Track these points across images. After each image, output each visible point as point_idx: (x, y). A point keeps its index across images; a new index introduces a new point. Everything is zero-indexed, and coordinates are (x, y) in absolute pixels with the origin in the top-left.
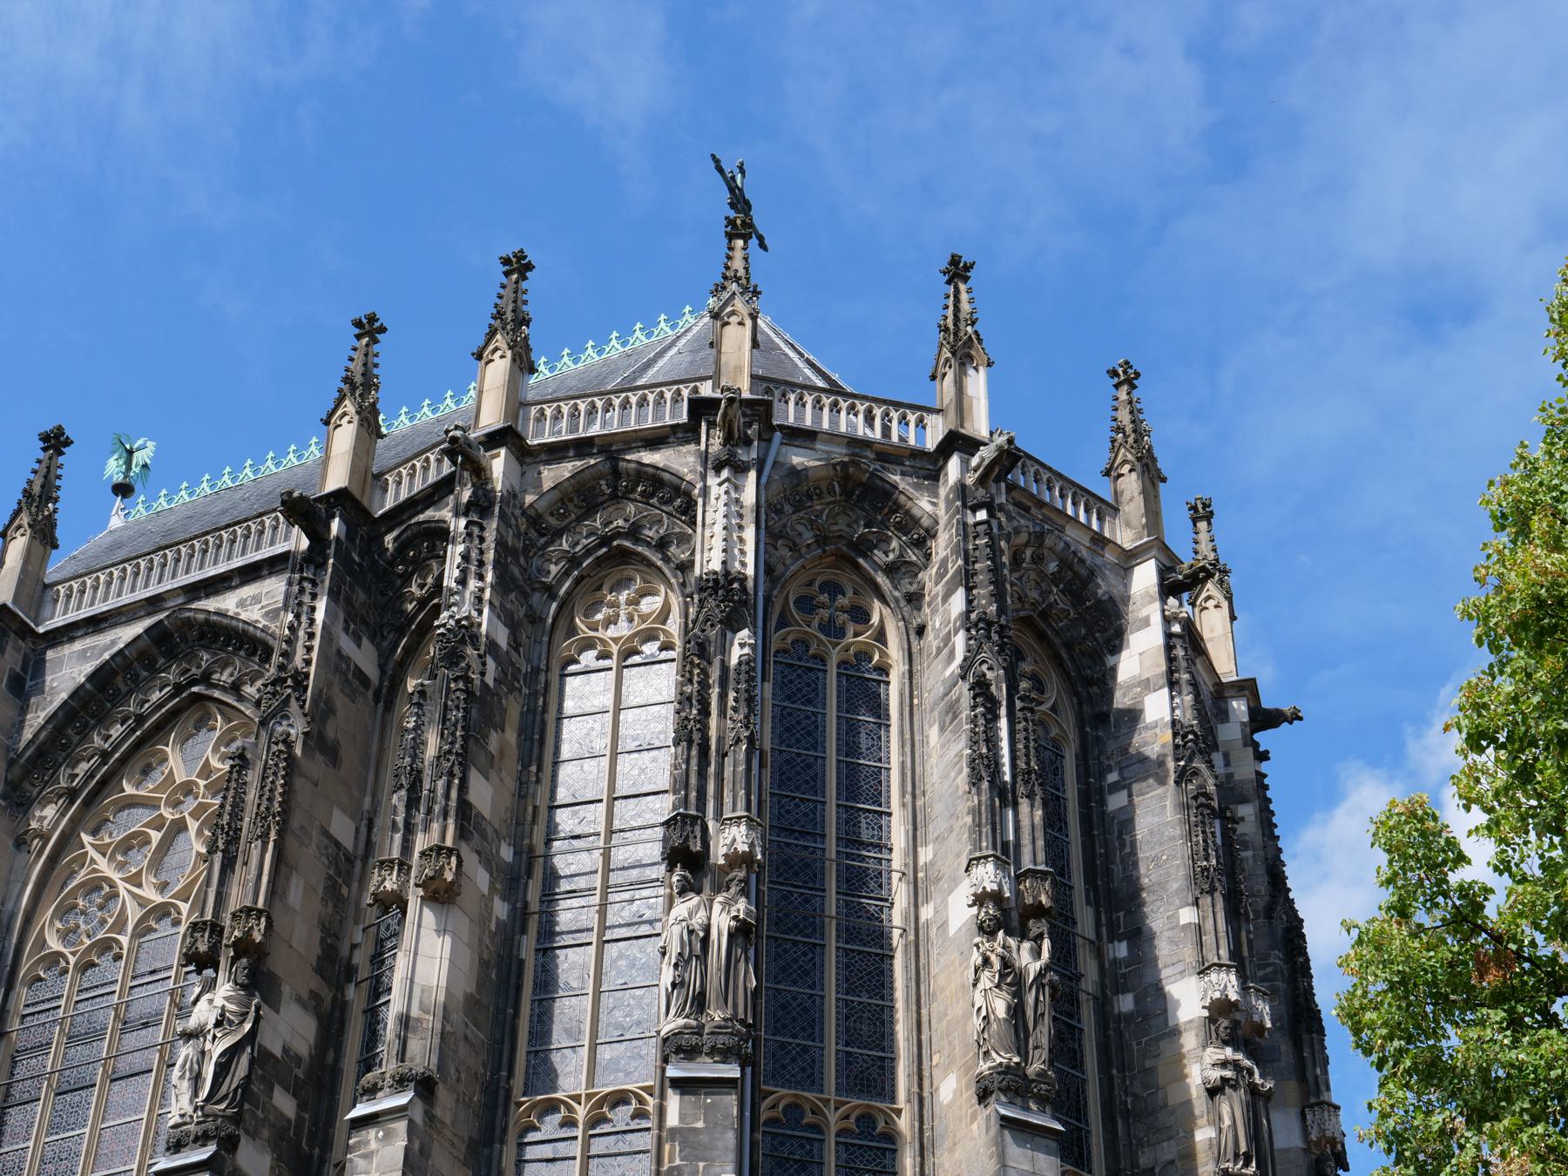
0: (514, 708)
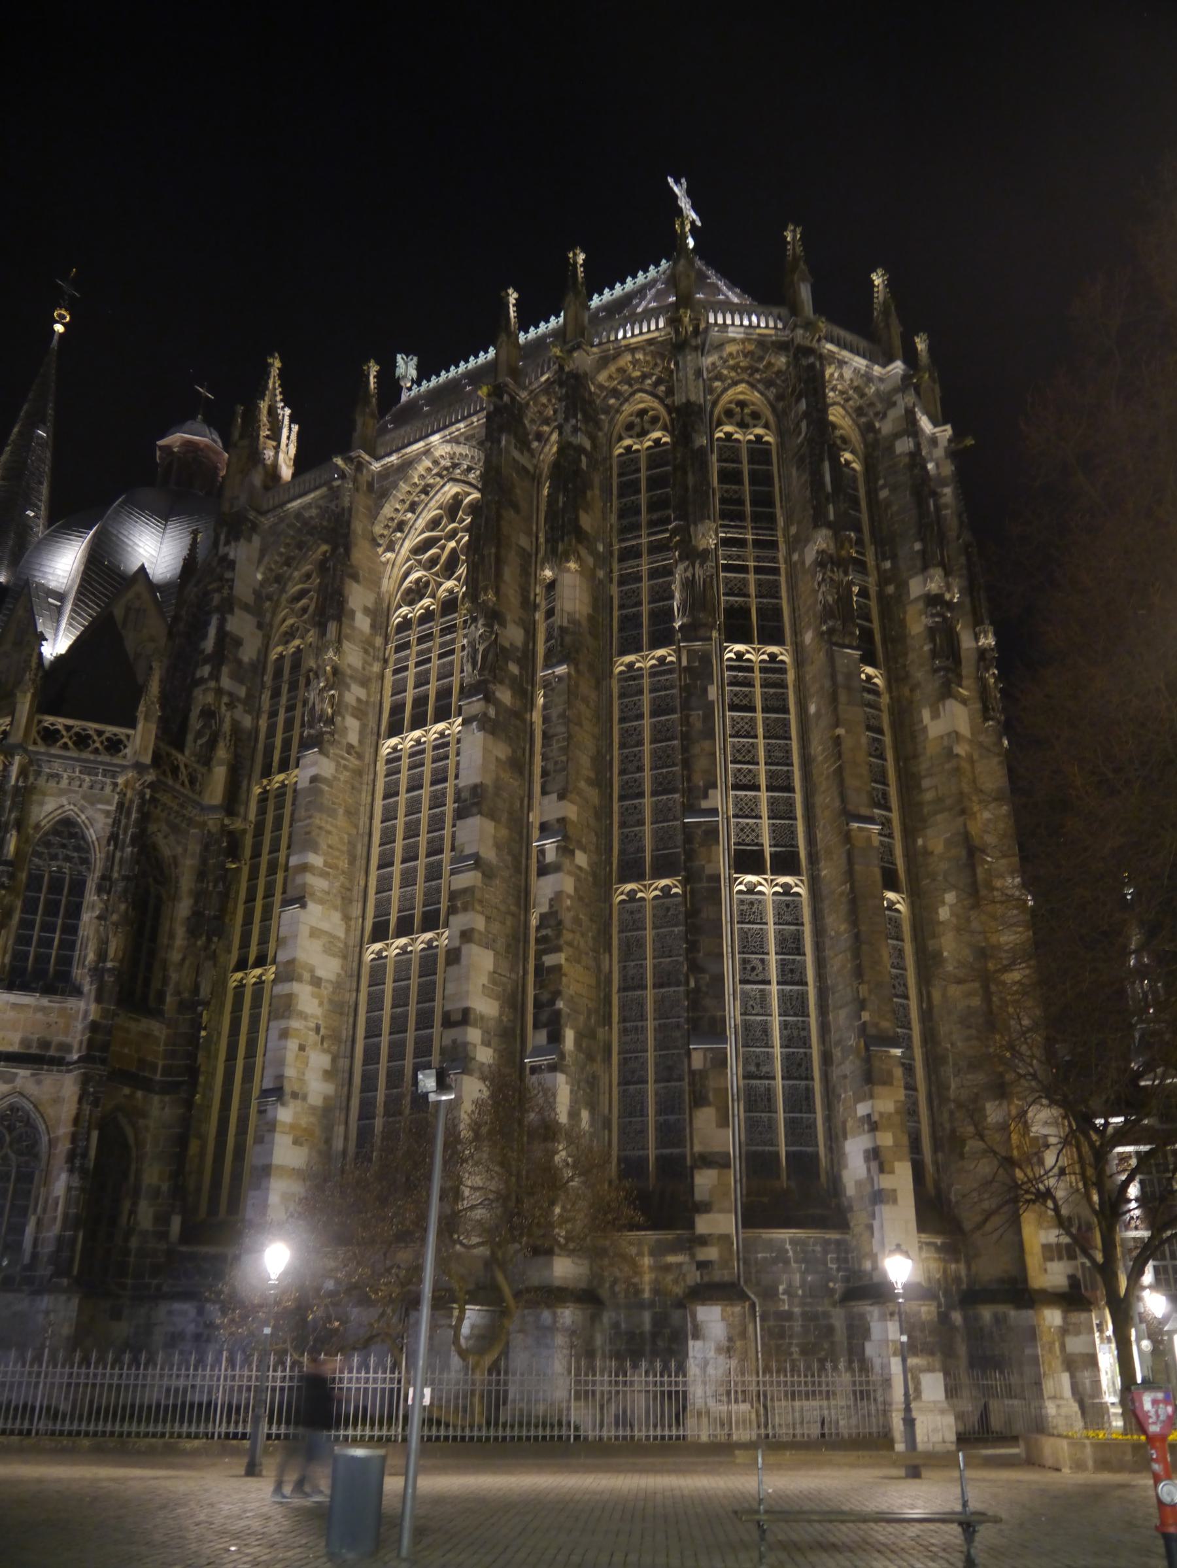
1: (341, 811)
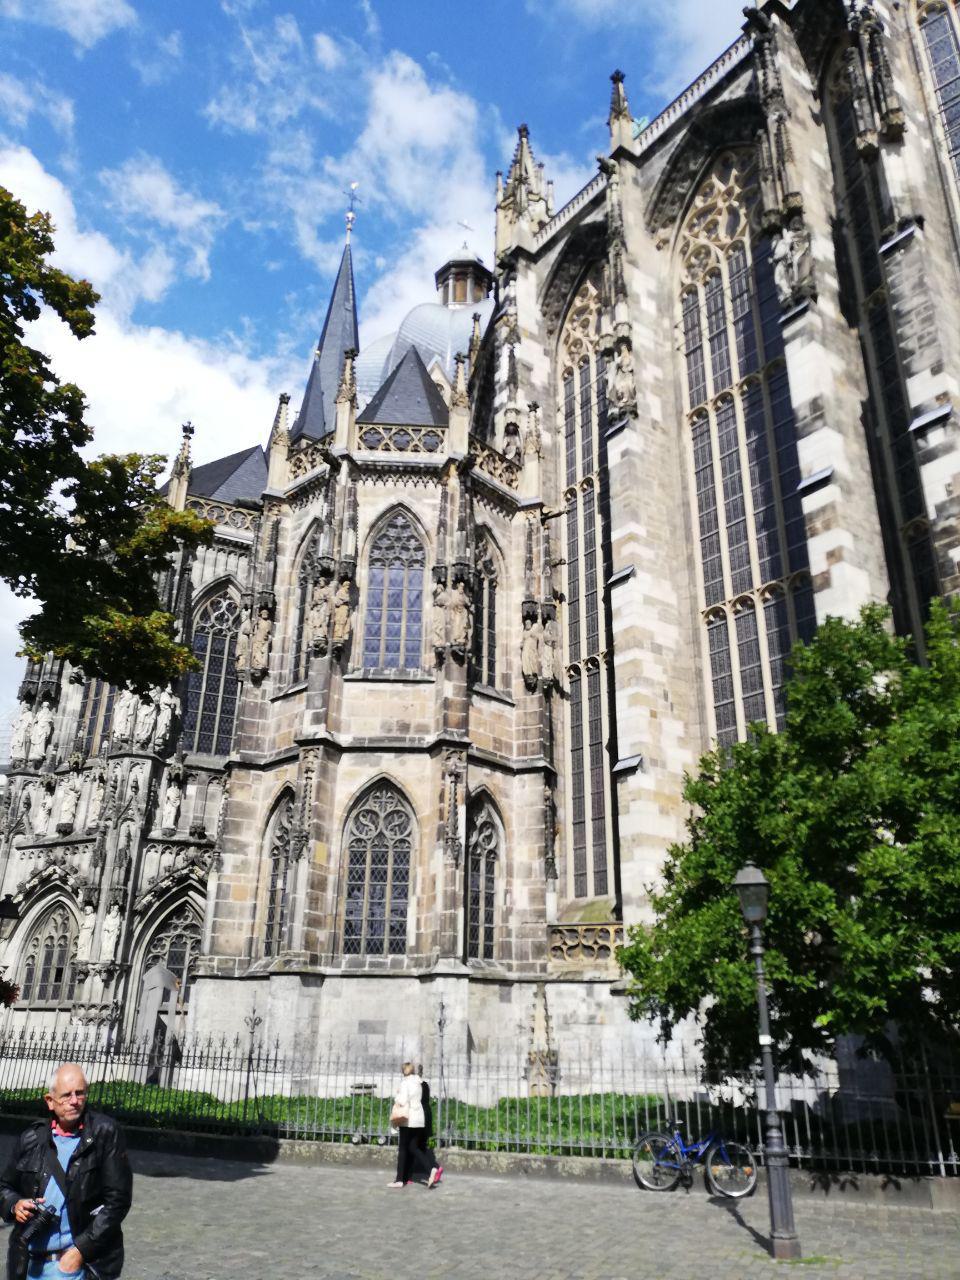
0: (902, 47)
1: (656, 483)
